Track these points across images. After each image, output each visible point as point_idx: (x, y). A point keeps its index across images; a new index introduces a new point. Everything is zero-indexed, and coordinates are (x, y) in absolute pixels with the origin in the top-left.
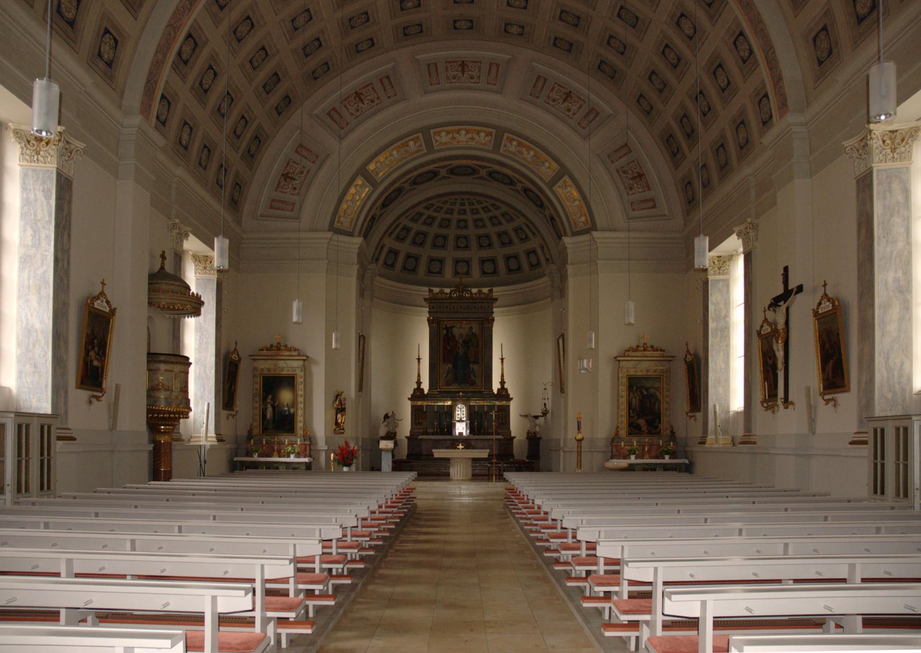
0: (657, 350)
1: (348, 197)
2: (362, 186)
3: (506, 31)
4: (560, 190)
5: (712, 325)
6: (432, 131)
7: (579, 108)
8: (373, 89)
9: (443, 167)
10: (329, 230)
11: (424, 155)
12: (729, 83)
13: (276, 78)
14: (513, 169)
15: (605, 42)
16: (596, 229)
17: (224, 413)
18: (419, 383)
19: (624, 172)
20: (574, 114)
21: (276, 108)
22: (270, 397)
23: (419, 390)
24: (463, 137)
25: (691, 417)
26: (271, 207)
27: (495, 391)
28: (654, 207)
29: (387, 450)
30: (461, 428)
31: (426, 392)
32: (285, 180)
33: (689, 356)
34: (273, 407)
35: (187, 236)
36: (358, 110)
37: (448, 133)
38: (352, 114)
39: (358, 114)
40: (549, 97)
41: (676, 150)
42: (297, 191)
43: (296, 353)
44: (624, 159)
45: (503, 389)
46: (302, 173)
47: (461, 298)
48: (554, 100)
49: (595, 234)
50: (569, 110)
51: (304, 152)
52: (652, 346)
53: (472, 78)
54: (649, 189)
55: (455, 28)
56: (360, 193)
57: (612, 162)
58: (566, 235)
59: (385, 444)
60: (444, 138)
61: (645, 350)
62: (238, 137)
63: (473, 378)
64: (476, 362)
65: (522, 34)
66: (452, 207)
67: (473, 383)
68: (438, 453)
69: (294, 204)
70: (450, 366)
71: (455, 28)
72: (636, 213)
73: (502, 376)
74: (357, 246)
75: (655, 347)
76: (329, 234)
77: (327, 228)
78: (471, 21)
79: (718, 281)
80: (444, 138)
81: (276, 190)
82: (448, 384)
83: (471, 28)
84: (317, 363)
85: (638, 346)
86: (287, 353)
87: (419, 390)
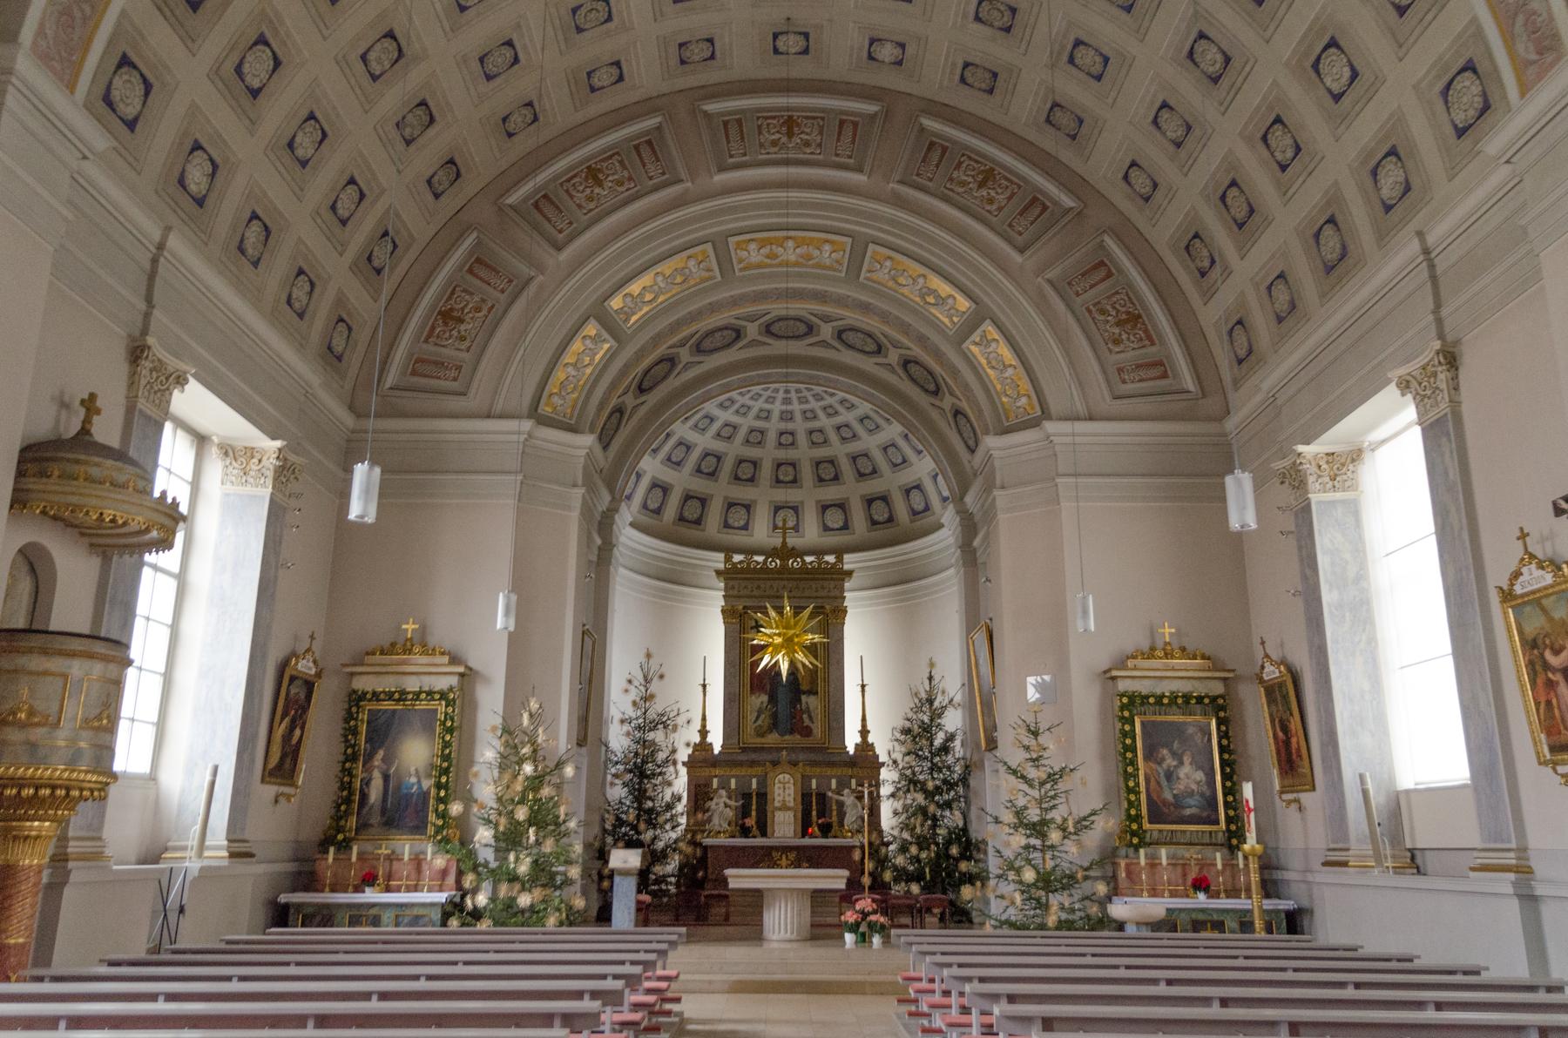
0: (1195, 658)
1: (569, 358)
2: (597, 339)
3: (871, 57)
4: (974, 349)
5: (1328, 597)
6: (732, 240)
7: (1010, 198)
8: (621, 162)
9: (752, 319)
10: (529, 417)
11: (717, 286)
12: (1298, 149)
13: (425, 111)
14: (885, 317)
15: (1065, 58)
16: (1050, 418)
17: (271, 790)
18: (704, 732)
19: (1103, 312)
20: (1000, 209)
21: (429, 182)
22: (381, 753)
23: (703, 746)
24: (790, 253)
25: (1289, 802)
26: (414, 373)
27: (851, 749)
28: (1164, 376)
29: (625, 873)
30: (784, 827)
31: (717, 749)
32: (446, 324)
33: (1269, 668)
34: (386, 778)
35: (181, 381)
36: (590, 199)
37: (763, 243)
38: (579, 206)
39: (592, 205)
40: (951, 179)
41: (1206, 263)
42: (467, 344)
43: (446, 659)
44: (1101, 287)
45: (865, 747)
46: (478, 310)
47: (784, 568)
48: (963, 184)
49: (1050, 426)
50: (991, 201)
51: (483, 273)
52: (1183, 649)
53: (807, 144)
54: (1153, 344)
55: (776, 51)
56: (590, 351)
57: (1078, 294)
58: (987, 432)
59: (625, 859)
60: (754, 255)
61: (1166, 656)
62: (344, 222)
63: (807, 722)
64: (812, 692)
65: (899, 63)
66: (767, 406)
67: (807, 732)
68: (740, 878)
69: (459, 368)
70: (764, 698)
71: (776, 51)
72: (1130, 387)
73: (864, 719)
74: (583, 452)
75: (1190, 648)
76: (527, 425)
77: (525, 410)
78: (806, 35)
79: (1333, 503)
80: (754, 255)
81: (426, 341)
82: (760, 733)
83: (806, 51)
84: (487, 680)
85: (1153, 649)
86: (424, 659)
87: (703, 746)
